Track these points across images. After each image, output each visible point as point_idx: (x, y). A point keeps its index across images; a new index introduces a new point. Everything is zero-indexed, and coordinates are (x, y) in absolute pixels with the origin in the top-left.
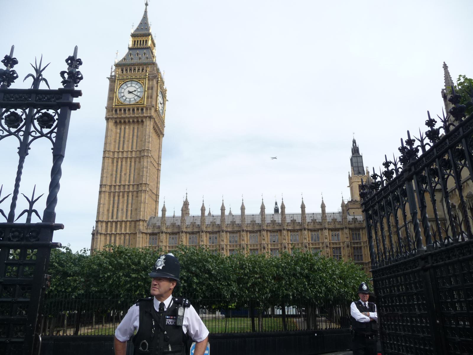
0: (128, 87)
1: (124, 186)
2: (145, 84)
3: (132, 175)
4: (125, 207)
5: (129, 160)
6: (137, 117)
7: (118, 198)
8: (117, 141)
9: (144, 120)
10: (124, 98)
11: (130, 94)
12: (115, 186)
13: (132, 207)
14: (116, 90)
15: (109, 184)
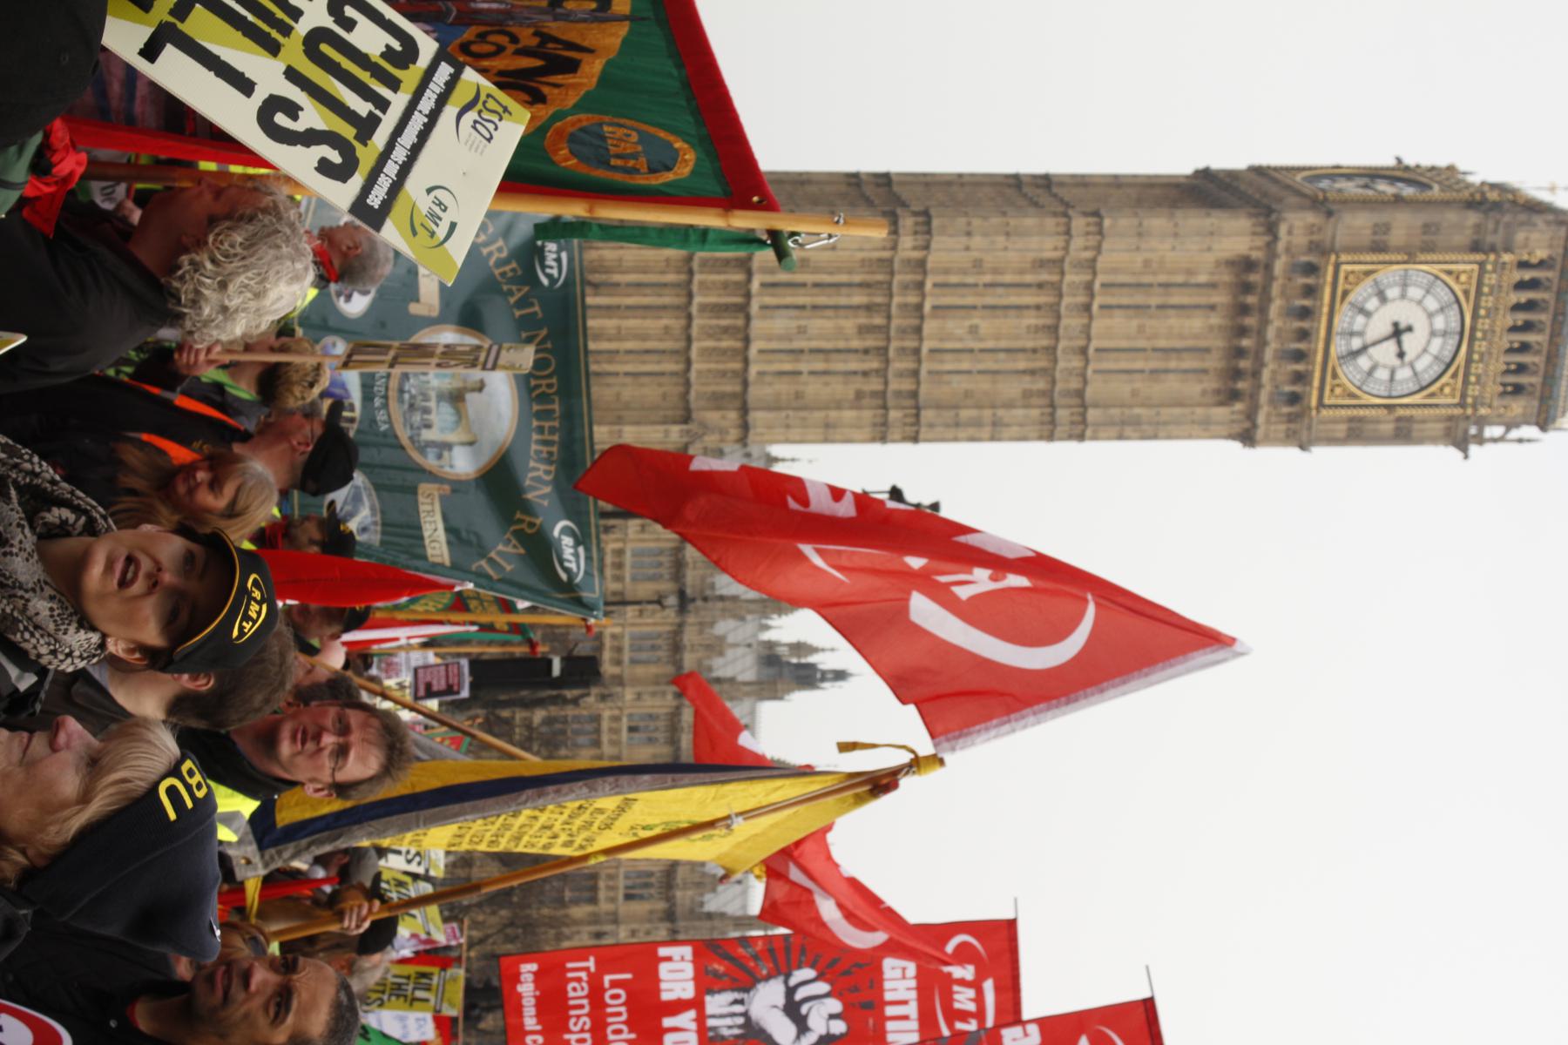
0: (1430, 315)
1: (918, 330)
2: (1430, 406)
3: (965, 366)
4: (814, 344)
5: (1045, 342)
6: (1256, 374)
7: (858, 307)
8: (1146, 279)
9: (1239, 406)
10: (1372, 304)
11: (1389, 329)
12: (920, 285)
13: (812, 373)
14: (1426, 263)
15: (933, 260)
